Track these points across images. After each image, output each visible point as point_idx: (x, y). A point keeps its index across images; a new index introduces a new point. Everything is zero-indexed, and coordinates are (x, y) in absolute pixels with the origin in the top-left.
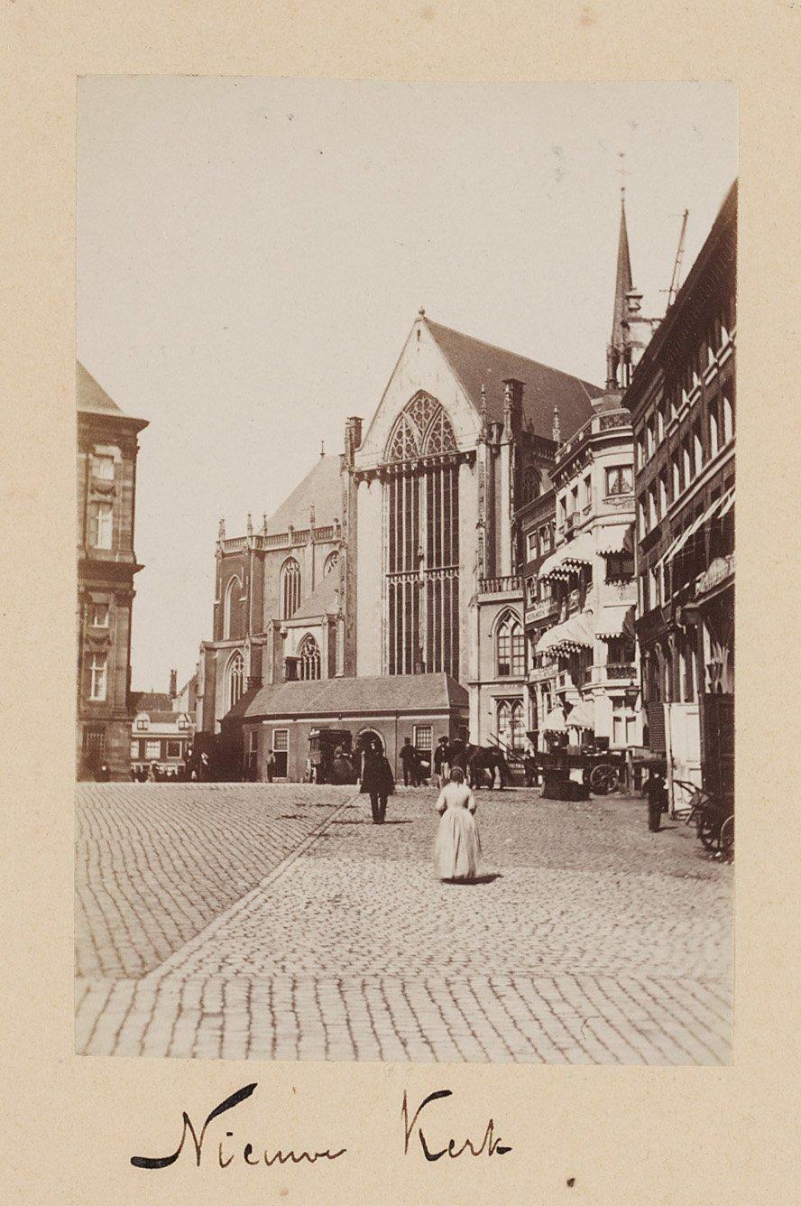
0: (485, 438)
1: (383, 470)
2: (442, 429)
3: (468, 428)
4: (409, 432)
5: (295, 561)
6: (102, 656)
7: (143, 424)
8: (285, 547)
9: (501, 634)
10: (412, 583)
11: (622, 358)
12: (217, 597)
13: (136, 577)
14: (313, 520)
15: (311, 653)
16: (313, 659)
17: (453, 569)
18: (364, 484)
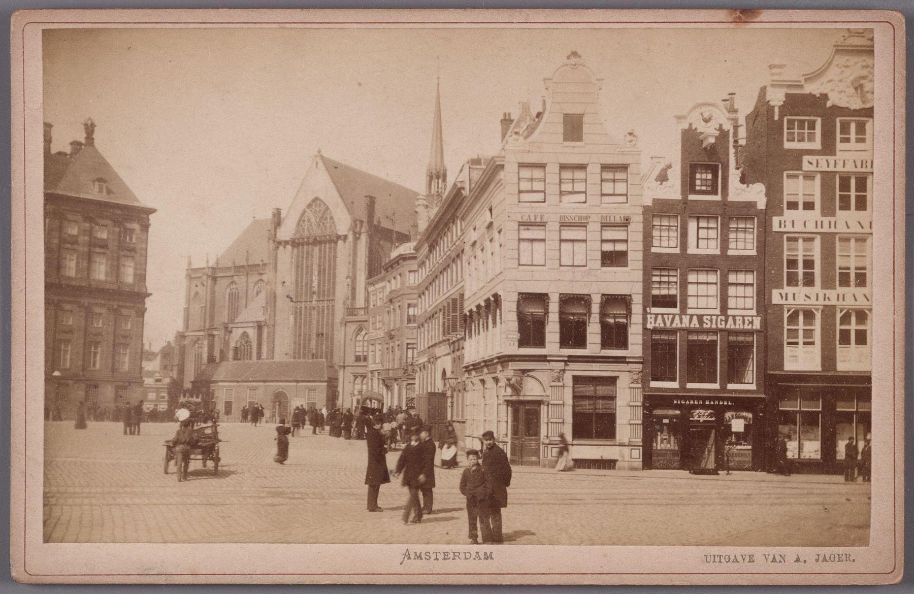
1: (293, 242)
2: (329, 220)
3: (343, 223)
4: (309, 220)
5: (236, 284)
6: (126, 346)
7: (153, 211)
8: (231, 275)
9: (358, 339)
11: (434, 177)
13: (147, 300)
15: (246, 343)
17: (332, 300)
18: (281, 248)
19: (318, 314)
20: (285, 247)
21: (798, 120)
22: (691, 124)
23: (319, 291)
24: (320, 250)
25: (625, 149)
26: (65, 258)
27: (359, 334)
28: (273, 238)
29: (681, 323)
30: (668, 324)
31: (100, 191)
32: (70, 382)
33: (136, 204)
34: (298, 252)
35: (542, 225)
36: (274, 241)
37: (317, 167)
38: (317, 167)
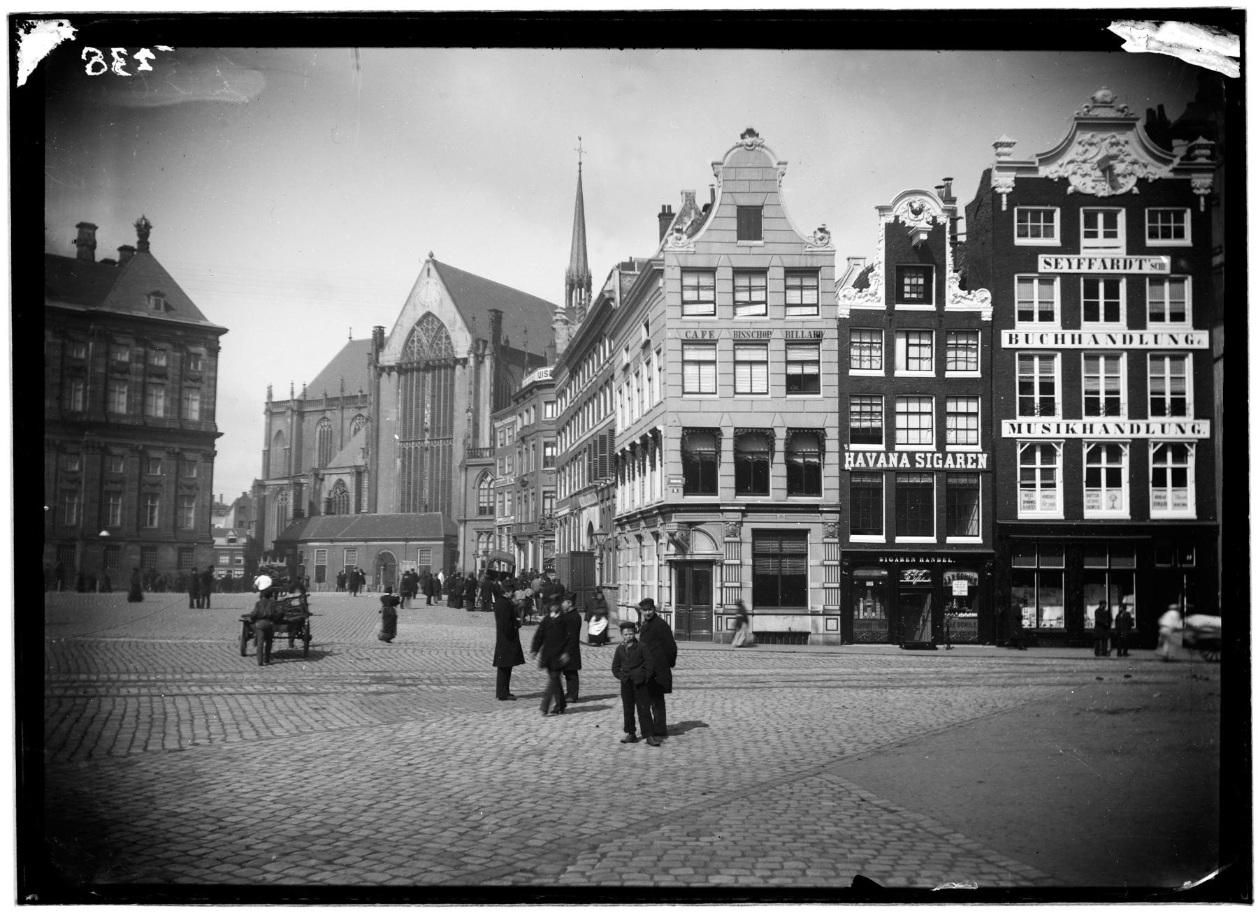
3: (462, 343)
4: (419, 340)
5: (328, 420)
6: (191, 498)
7: (224, 331)
11: (576, 286)
13: (218, 441)
18: (385, 375)
19: (432, 455)
20: (389, 374)
21: (1031, 210)
22: (897, 217)
23: (433, 429)
24: (433, 377)
25: (816, 249)
26: (114, 391)
28: (374, 362)
29: (888, 462)
30: (871, 464)
31: (157, 307)
32: (122, 544)
33: (202, 323)
34: (406, 380)
35: (712, 343)
36: (376, 367)
37: (428, 275)
38: (428, 275)
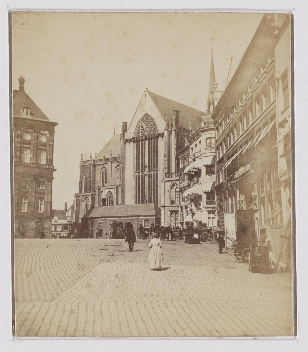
0: (167, 129)
1: (134, 139)
2: (153, 126)
3: (161, 126)
4: (142, 127)
5: (105, 168)
6: (42, 198)
7: (56, 124)
8: (103, 163)
9: (172, 191)
10: (143, 175)
11: (211, 103)
12: (80, 180)
14: (111, 155)
15: (110, 197)
16: (111, 199)
17: (156, 170)
18: (127, 143)
19: (149, 178)
23: (149, 166)
27: (172, 188)
31: (27, 114)
36: (123, 140)
